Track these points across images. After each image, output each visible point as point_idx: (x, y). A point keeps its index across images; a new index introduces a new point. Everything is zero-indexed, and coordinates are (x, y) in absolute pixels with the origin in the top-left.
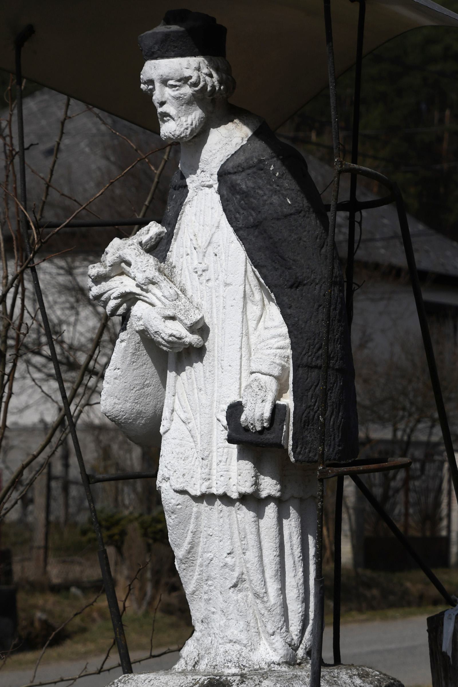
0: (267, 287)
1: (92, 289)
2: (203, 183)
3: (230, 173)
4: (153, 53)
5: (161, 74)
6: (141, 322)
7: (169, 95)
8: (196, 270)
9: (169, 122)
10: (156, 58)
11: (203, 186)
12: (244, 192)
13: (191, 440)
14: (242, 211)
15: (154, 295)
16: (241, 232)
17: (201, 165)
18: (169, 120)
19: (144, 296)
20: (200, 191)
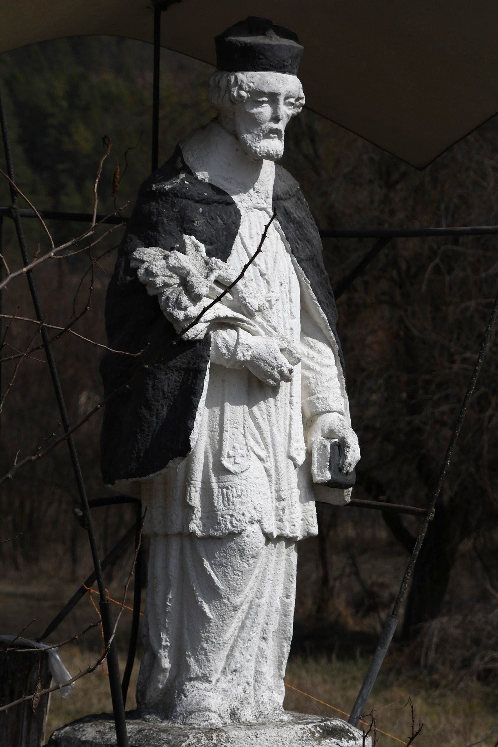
0: (328, 324)
1: (188, 309)
2: (257, 205)
3: (281, 199)
4: (284, 66)
5: (289, 90)
6: (250, 353)
7: (284, 113)
8: (269, 299)
9: (274, 139)
10: (284, 72)
11: (254, 208)
12: (298, 222)
13: (266, 479)
14: (299, 242)
15: (259, 323)
16: (304, 264)
17: (257, 185)
18: (275, 137)
19: (248, 324)
20: (250, 212)
